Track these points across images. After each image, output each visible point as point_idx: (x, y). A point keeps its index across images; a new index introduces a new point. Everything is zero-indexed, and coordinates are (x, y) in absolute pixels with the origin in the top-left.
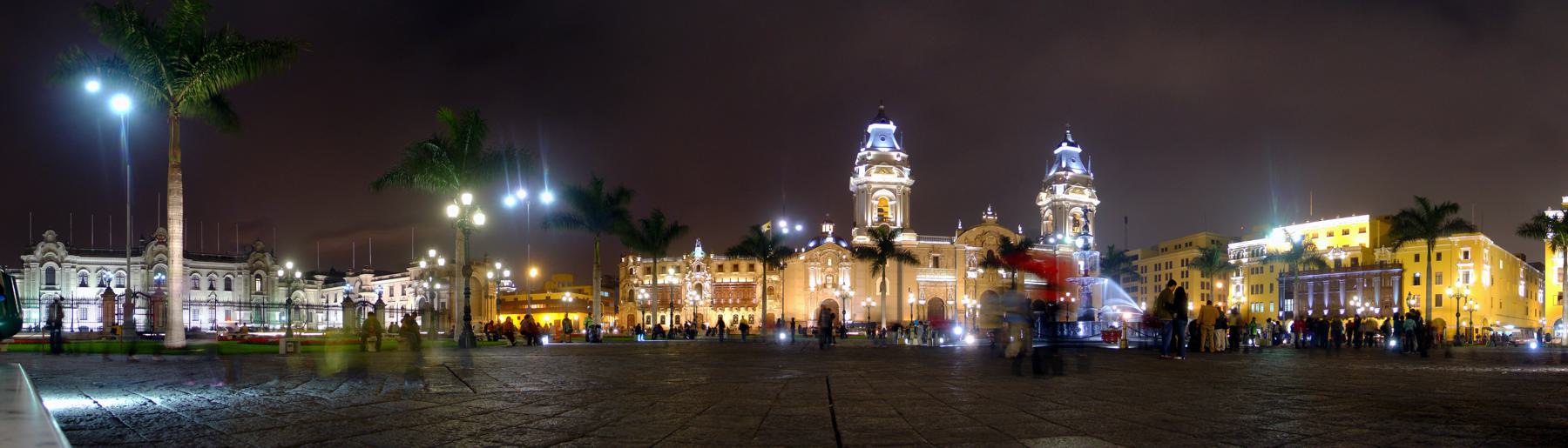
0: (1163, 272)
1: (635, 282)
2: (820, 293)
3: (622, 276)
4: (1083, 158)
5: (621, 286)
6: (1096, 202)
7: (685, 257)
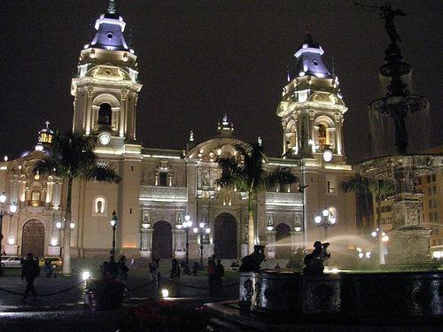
4: (326, 61)
6: (344, 110)
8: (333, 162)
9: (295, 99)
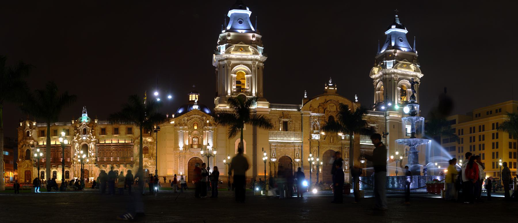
0: (477, 134)
1: (31, 143)
2: (188, 151)
3: (20, 138)
4: (409, 38)
5: (19, 146)
6: (420, 75)
7: (73, 123)
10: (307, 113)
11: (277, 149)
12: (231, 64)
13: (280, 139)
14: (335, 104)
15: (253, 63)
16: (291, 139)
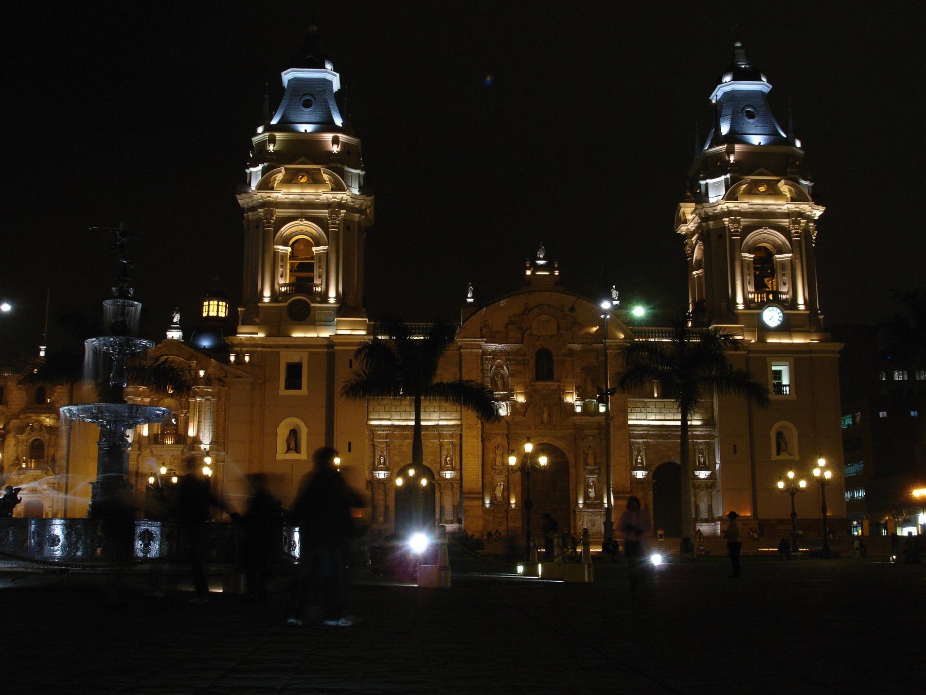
8: (785, 328)
9: (701, 198)
10: (474, 345)
11: (391, 446)
12: (274, 218)
13: (399, 418)
14: (554, 317)
15: (331, 213)
16: (431, 418)
